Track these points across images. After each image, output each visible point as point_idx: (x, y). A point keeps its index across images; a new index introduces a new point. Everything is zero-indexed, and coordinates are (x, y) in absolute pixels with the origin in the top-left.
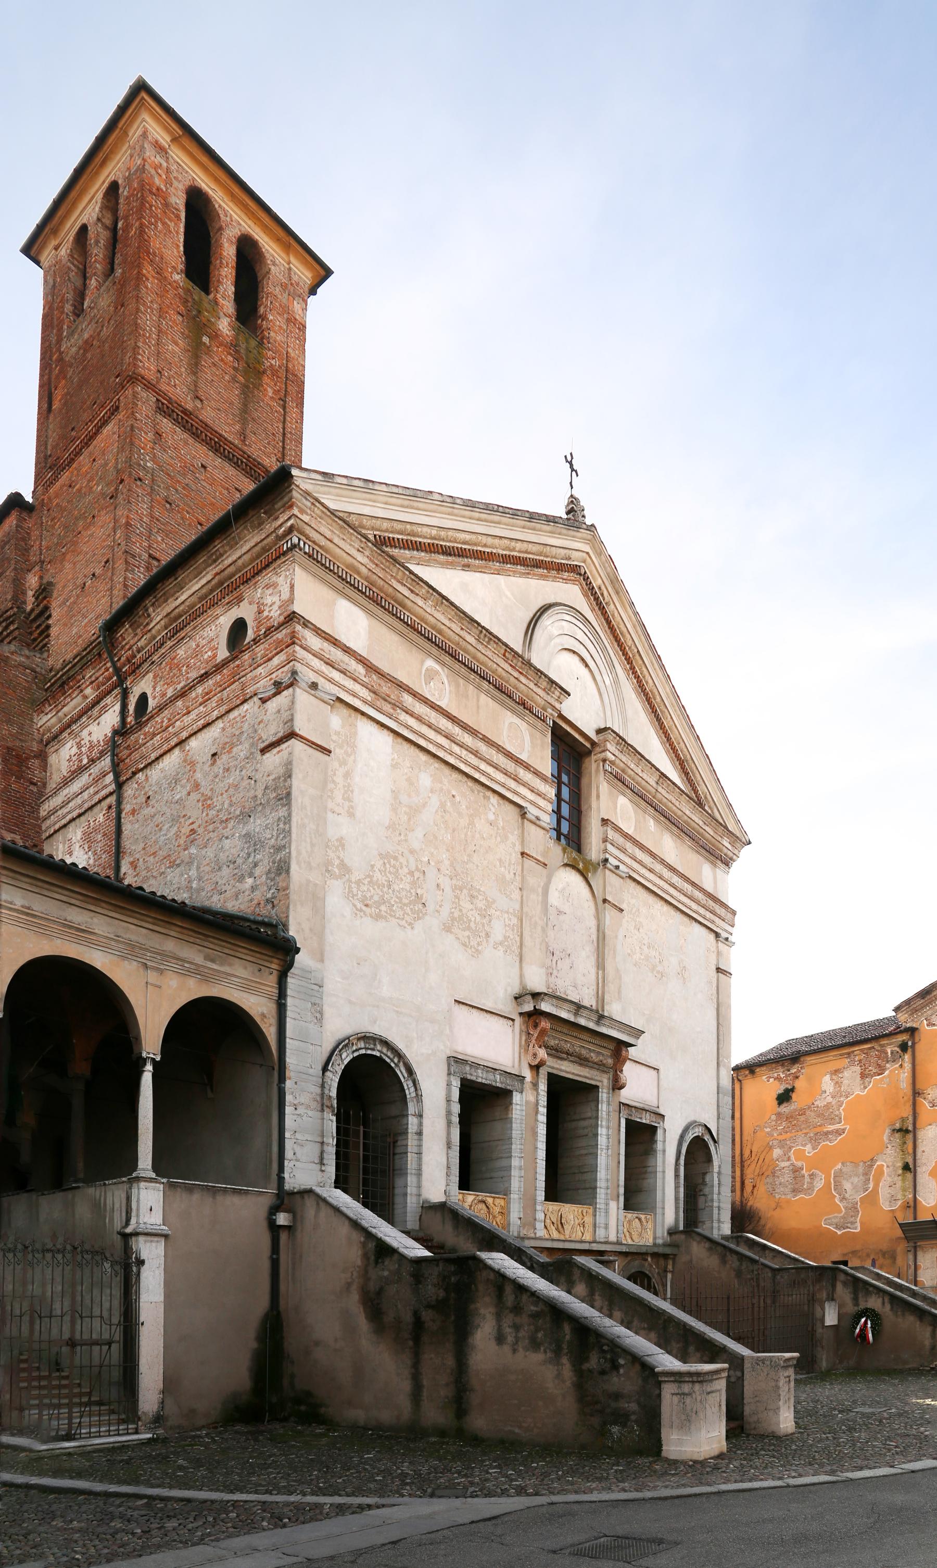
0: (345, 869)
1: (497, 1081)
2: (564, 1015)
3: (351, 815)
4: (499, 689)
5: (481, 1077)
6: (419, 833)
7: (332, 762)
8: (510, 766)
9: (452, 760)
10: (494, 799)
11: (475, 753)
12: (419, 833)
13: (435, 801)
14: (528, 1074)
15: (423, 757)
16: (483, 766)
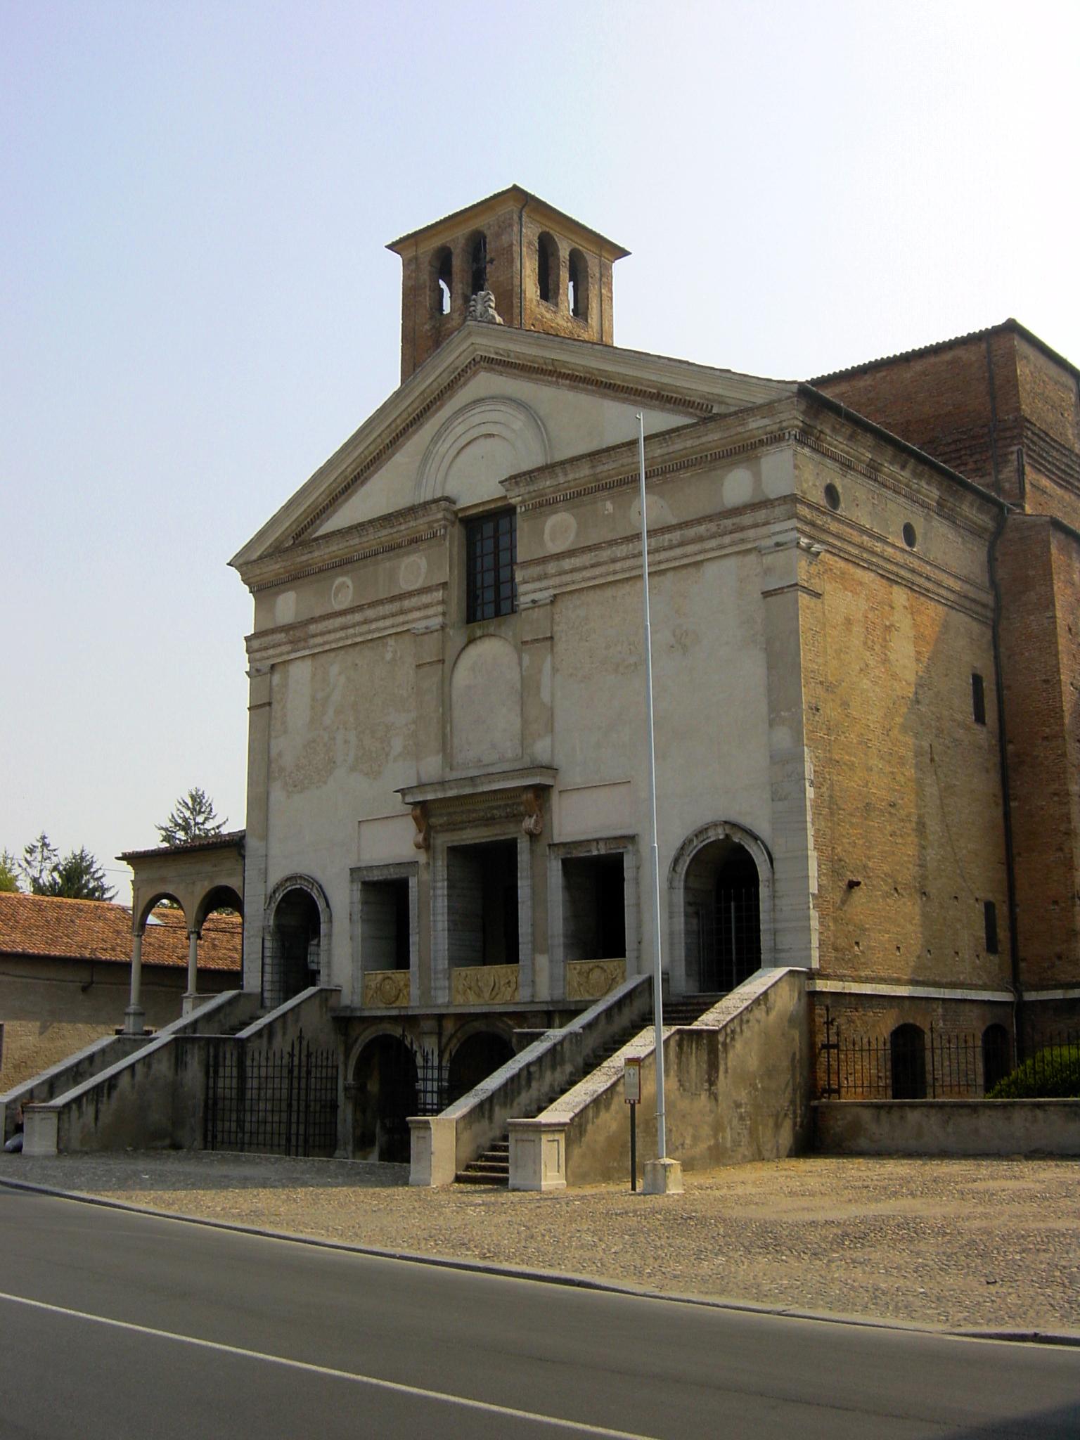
0: (282, 769)
1: (393, 874)
2: (430, 797)
3: (285, 732)
4: (392, 549)
5: (376, 876)
6: (331, 712)
7: (275, 706)
8: (395, 607)
9: (349, 642)
10: (391, 642)
11: (366, 622)
12: (331, 712)
13: (342, 679)
14: (422, 858)
15: (332, 654)
16: (374, 626)
